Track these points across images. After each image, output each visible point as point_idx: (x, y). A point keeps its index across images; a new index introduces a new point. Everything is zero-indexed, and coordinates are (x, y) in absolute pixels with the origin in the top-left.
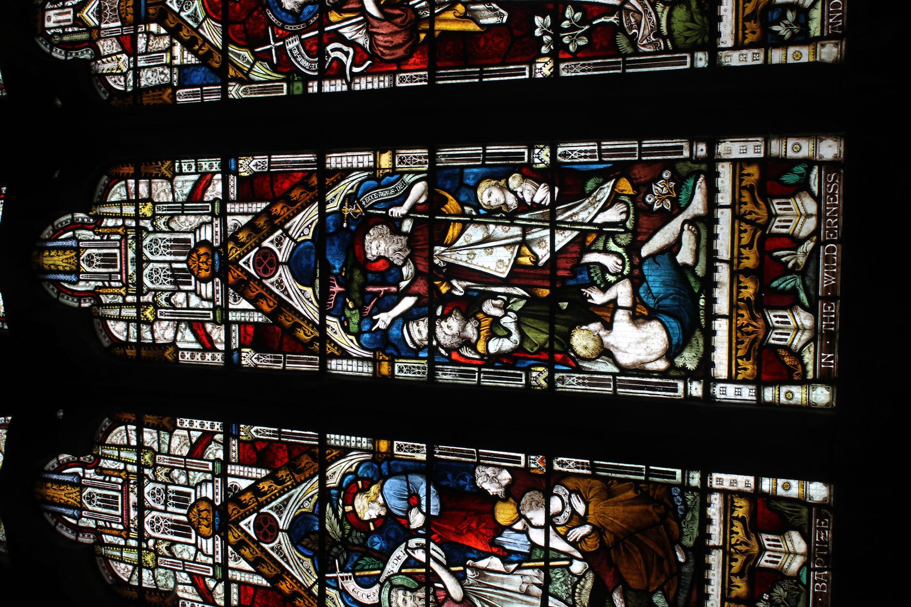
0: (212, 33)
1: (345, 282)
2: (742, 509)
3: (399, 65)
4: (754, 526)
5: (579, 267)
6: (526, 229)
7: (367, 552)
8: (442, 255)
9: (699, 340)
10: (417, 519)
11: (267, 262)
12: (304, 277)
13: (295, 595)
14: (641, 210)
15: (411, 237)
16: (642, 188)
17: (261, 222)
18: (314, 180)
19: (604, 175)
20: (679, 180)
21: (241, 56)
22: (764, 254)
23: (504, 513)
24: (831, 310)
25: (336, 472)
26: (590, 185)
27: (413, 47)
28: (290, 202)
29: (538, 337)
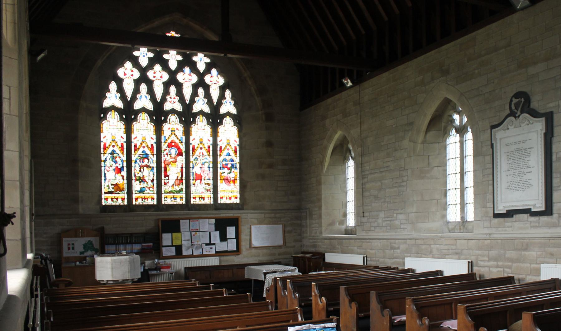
0: (169, 141)
1: (142, 157)
2: (123, 197)
3: (164, 163)
4: (122, 198)
5: (144, 182)
6: (148, 177)
7: (113, 160)
8: (145, 168)
9: (139, 193)
10: (117, 165)
11: (144, 147)
12: (143, 152)
13: (106, 150)
14: (150, 188)
15: (147, 165)
16: (152, 188)
17: (148, 147)
18: (153, 153)
19: (153, 184)
20: (153, 191)
21: (167, 144)
22: (146, 198)
23: (119, 174)
24: (141, 204)
25: (121, 155)
26: (152, 183)
27: (166, 165)
28: (151, 150)
29: (137, 178)
